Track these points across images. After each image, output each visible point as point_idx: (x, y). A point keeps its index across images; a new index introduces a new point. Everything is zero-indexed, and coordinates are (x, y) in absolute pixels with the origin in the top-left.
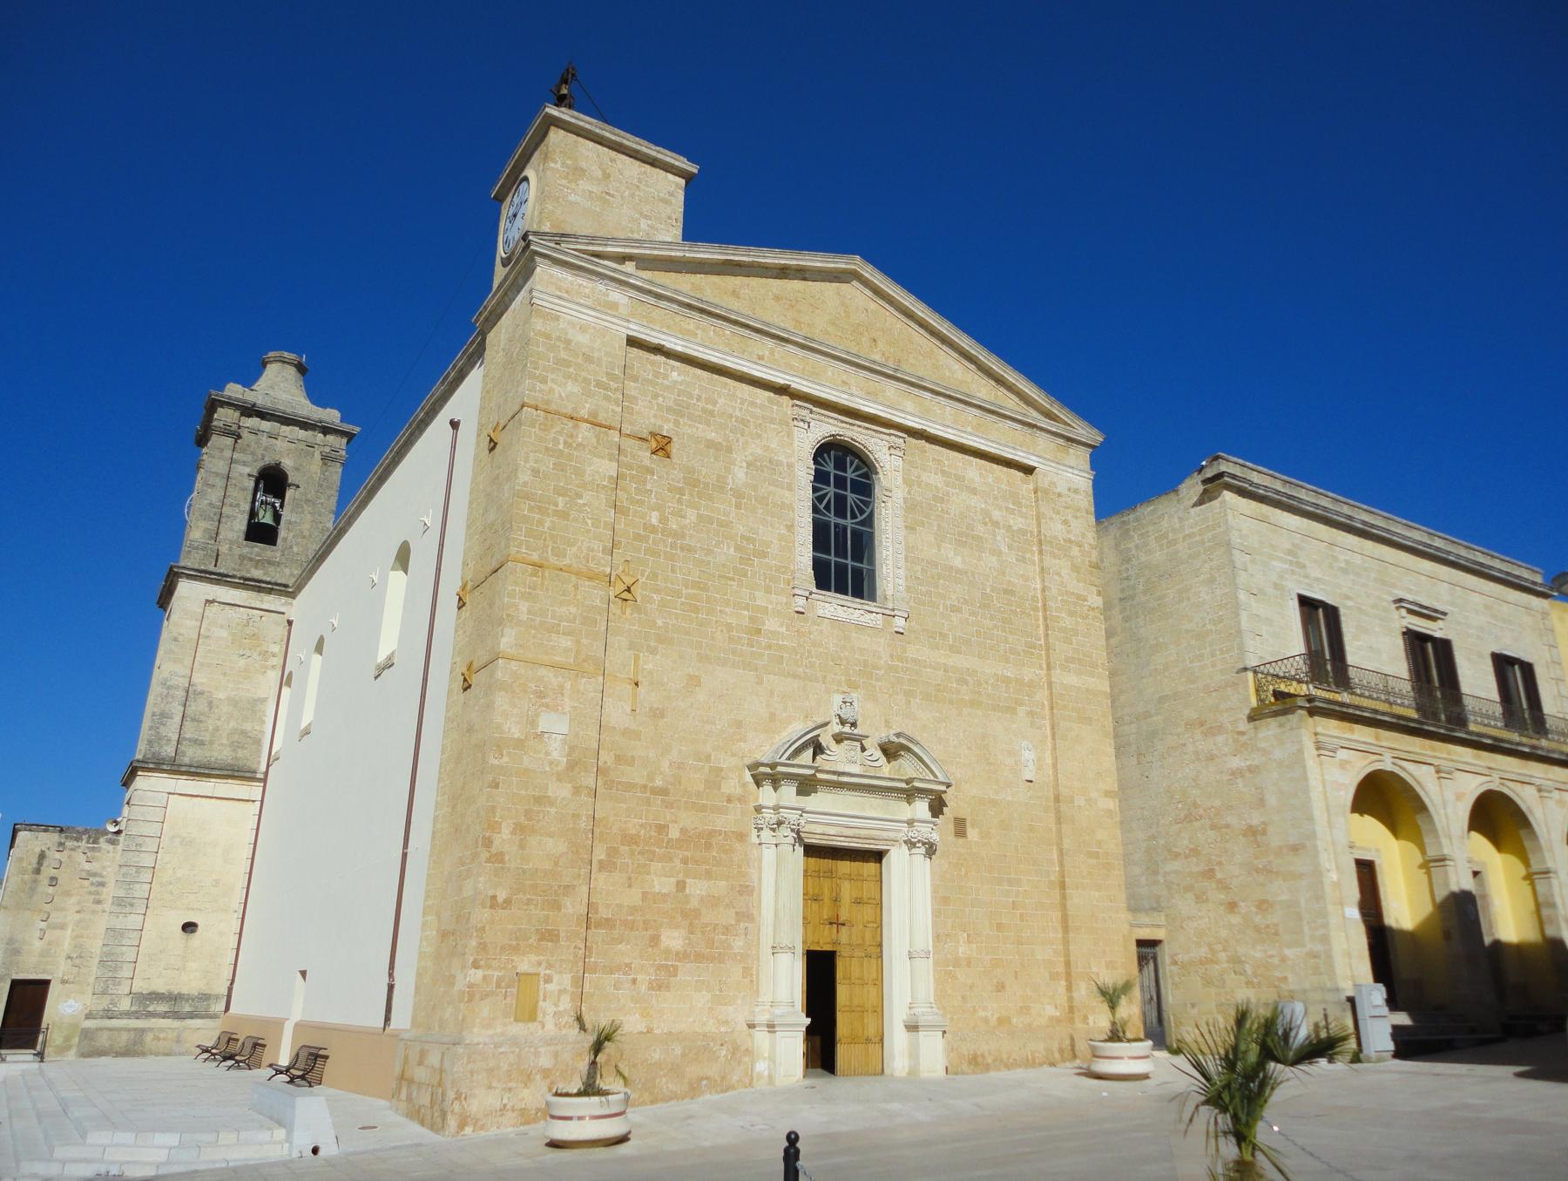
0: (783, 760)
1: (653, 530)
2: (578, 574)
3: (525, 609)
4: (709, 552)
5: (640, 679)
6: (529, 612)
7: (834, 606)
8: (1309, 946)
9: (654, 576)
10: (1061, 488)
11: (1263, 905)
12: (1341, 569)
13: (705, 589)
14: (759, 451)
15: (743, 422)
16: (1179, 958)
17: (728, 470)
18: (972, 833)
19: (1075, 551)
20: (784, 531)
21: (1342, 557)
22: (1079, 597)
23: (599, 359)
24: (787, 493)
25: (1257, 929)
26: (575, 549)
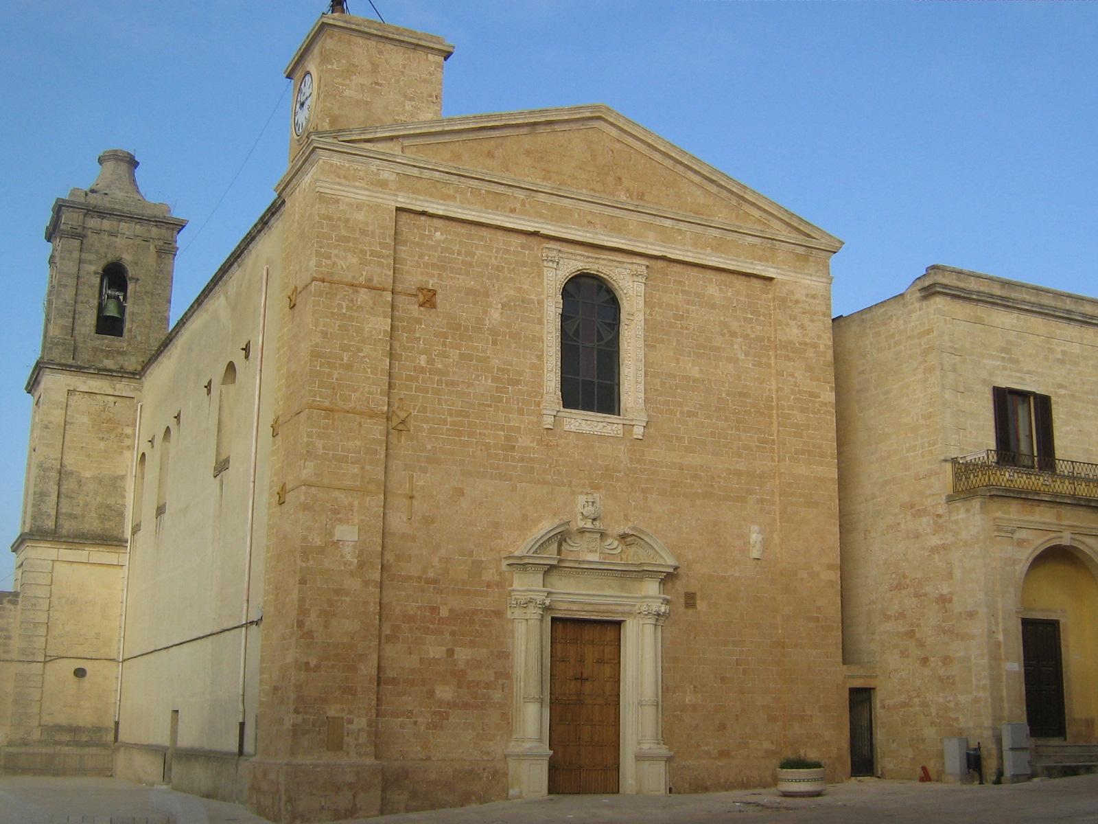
0: (530, 554)
1: (423, 370)
2: (361, 413)
3: (320, 446)
4: (470, 385)
5: (415, 493)
6: (324, 448)
7: (582, 422)
8: (975, 694)
9: (424, 409)
10: (800, 294)
11: (946, 660)
12: (1058, 360)
13: (467, 415)
14: (512, 293)
15: (498, 268)
16: (886, 702)
17: (485, 312)
18: (701, 605)
19: (810, 353)
20: (535, 361)
21: (1059, 349)
22: (811, 394)
23: (373, 233)
24: (538, 327)
25: (941, 679)
26: (357, 394)
